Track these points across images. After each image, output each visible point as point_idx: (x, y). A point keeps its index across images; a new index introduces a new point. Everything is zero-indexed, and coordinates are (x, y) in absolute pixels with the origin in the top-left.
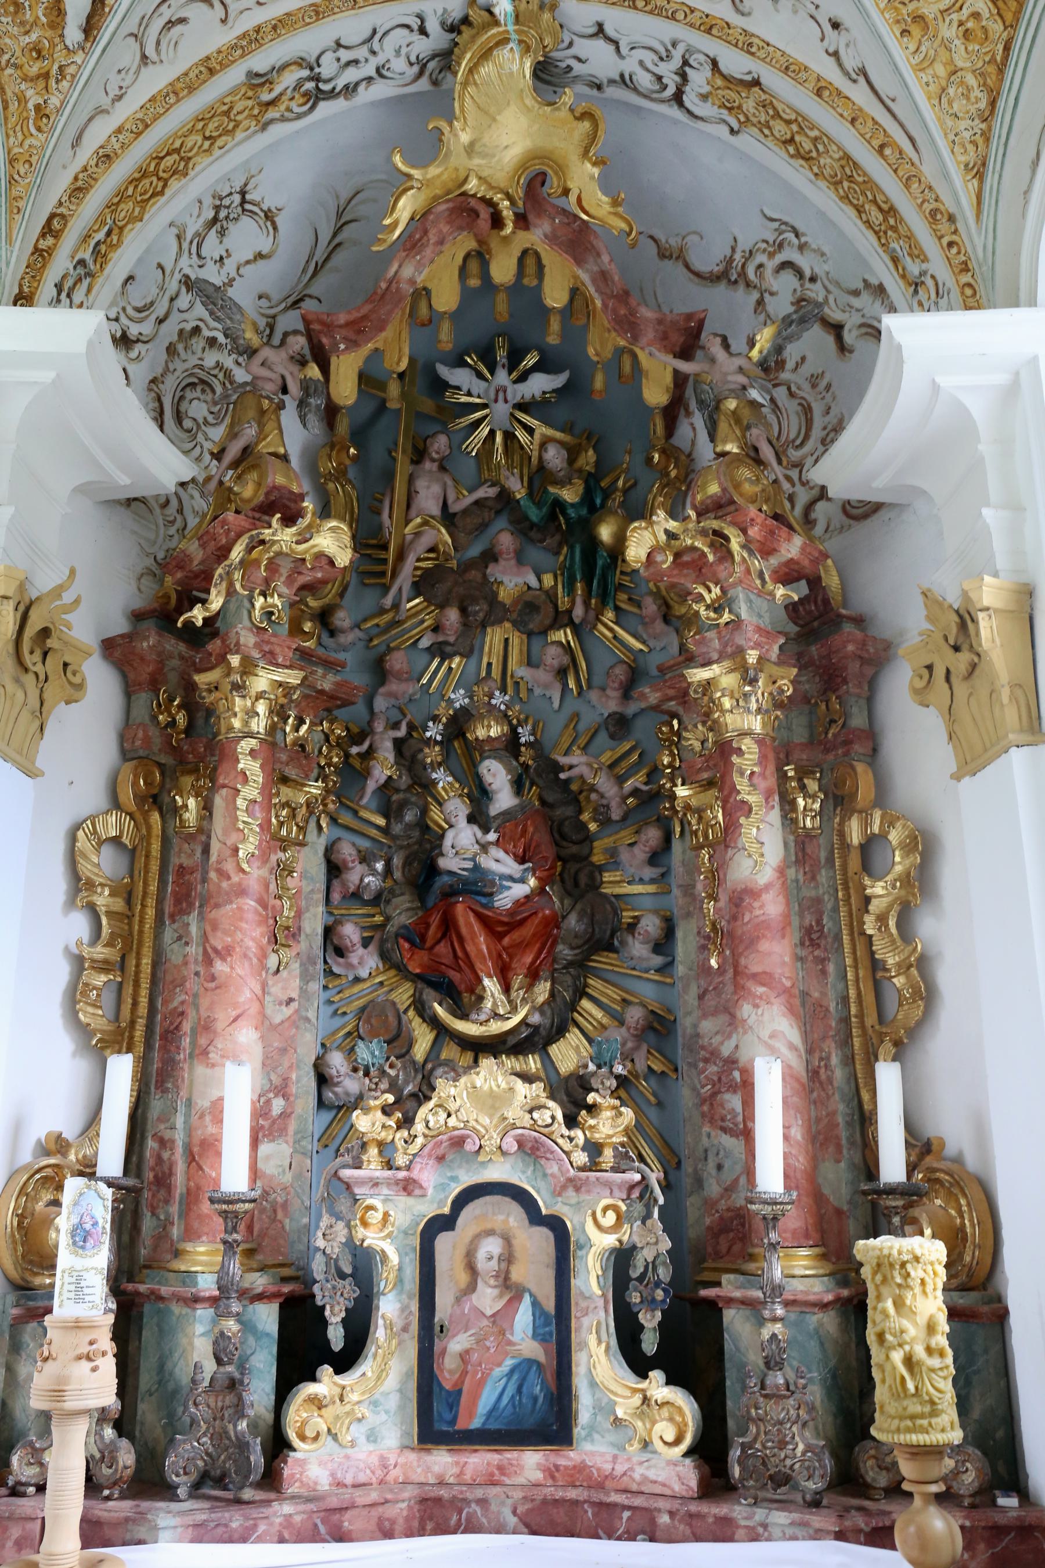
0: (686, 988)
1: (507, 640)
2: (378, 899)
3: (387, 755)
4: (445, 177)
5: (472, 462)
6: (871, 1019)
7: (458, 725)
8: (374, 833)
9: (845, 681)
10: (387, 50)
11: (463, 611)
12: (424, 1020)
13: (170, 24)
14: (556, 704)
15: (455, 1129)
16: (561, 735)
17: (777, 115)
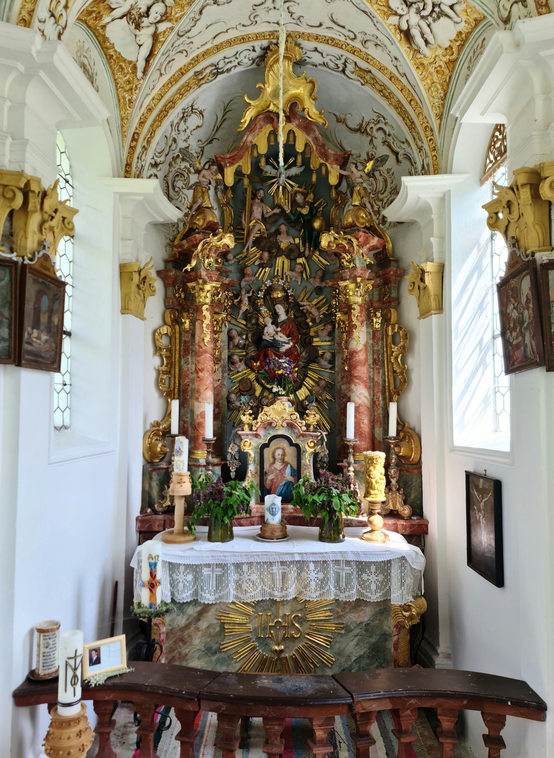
0: (338, 375)
2: (244, 347)
4: (262, 104)
5: (272, 198)
6: (392, 387)
9: (390, 282)
10: (241, 57)
11: (270, 252)
13: (170, 62)
17: (377, 82)
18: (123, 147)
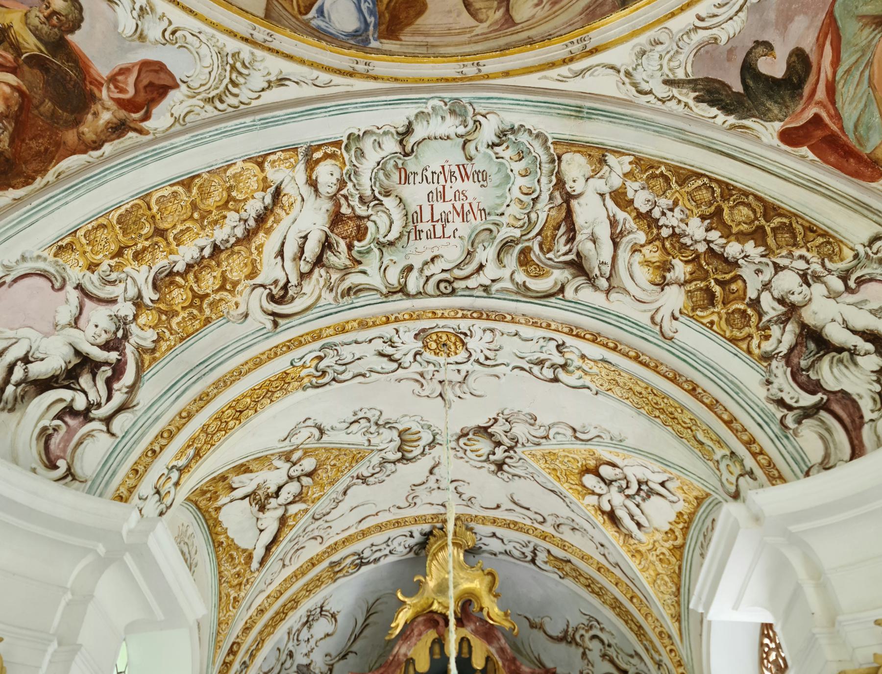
4: (422, 602)
13: (298, 550)
17: (580, 575)
18: (214, 663)
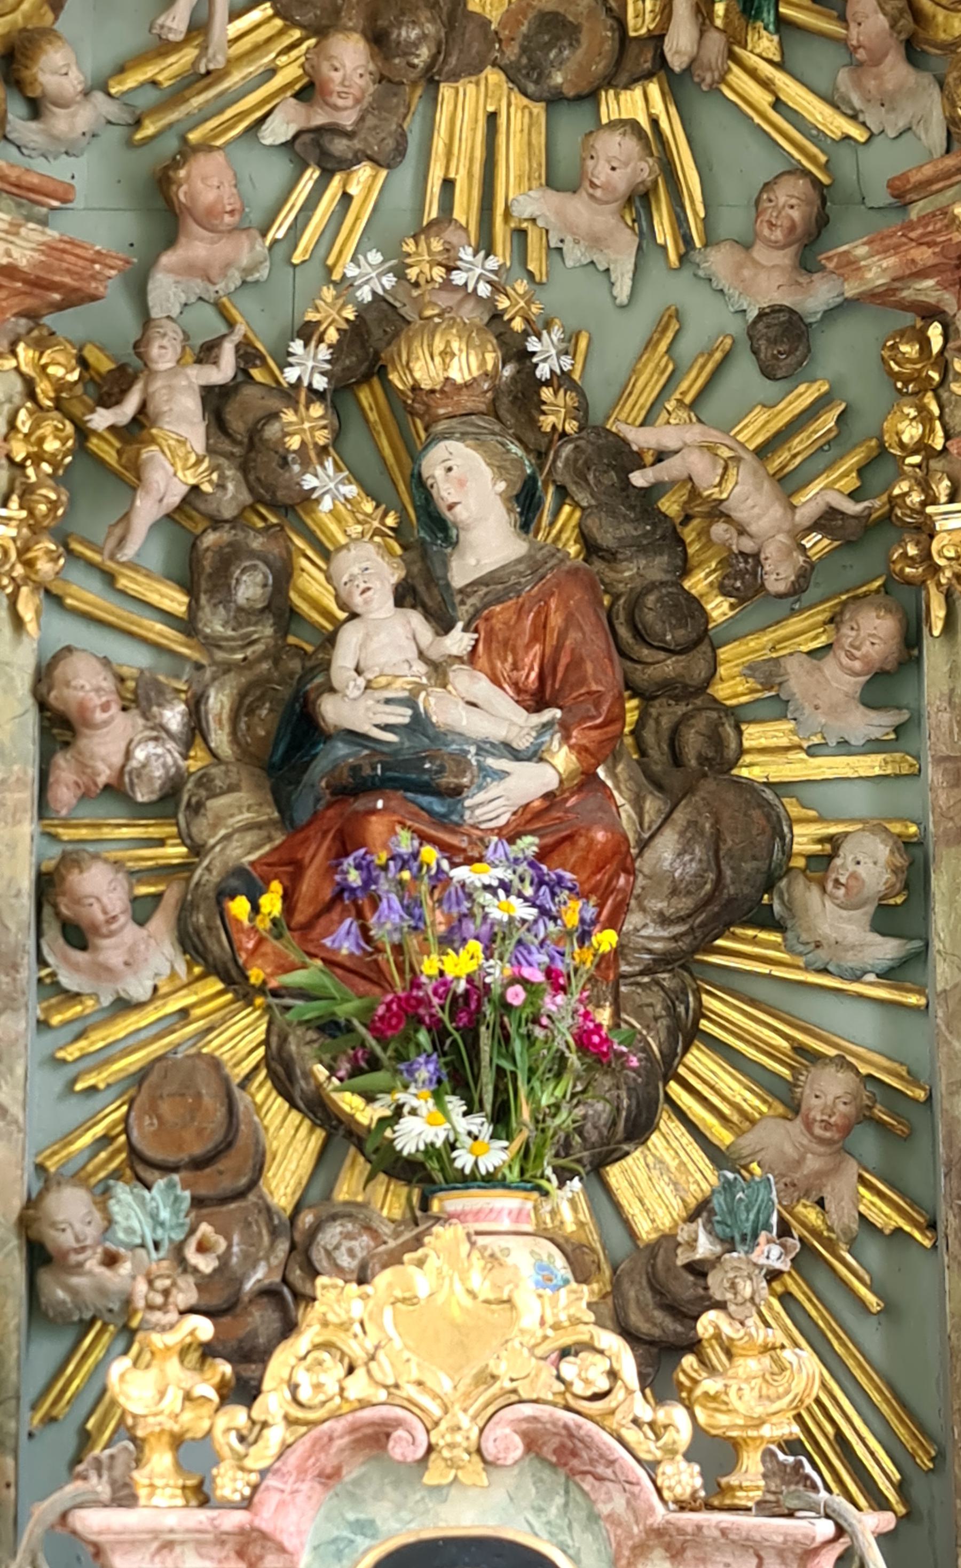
1: (492, 118)
2: (172, 800)
3: (184, 431)
7: (369, 346)
8: (158, 630)
11: (378, 40)
12: (293, 1105)
14: (623, 290)
15: (364, 1404)
16: (634, 371)
